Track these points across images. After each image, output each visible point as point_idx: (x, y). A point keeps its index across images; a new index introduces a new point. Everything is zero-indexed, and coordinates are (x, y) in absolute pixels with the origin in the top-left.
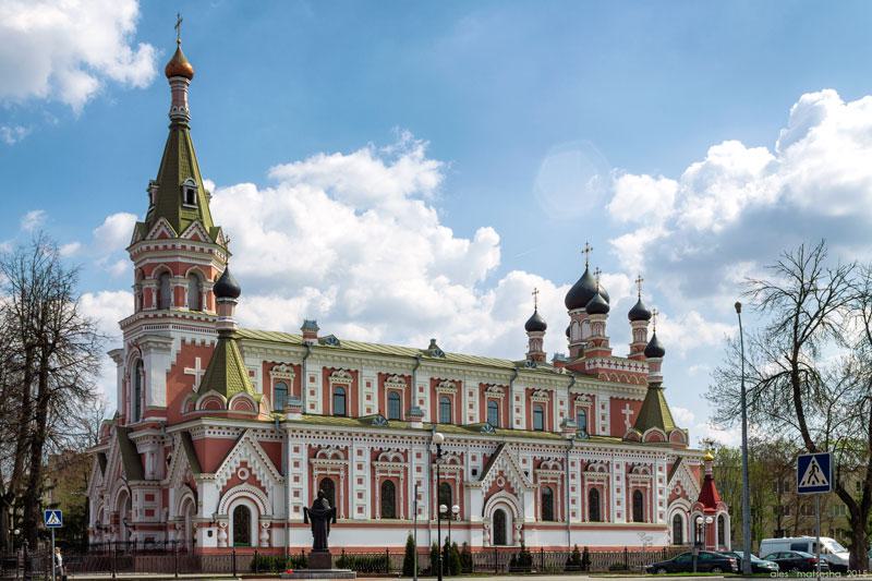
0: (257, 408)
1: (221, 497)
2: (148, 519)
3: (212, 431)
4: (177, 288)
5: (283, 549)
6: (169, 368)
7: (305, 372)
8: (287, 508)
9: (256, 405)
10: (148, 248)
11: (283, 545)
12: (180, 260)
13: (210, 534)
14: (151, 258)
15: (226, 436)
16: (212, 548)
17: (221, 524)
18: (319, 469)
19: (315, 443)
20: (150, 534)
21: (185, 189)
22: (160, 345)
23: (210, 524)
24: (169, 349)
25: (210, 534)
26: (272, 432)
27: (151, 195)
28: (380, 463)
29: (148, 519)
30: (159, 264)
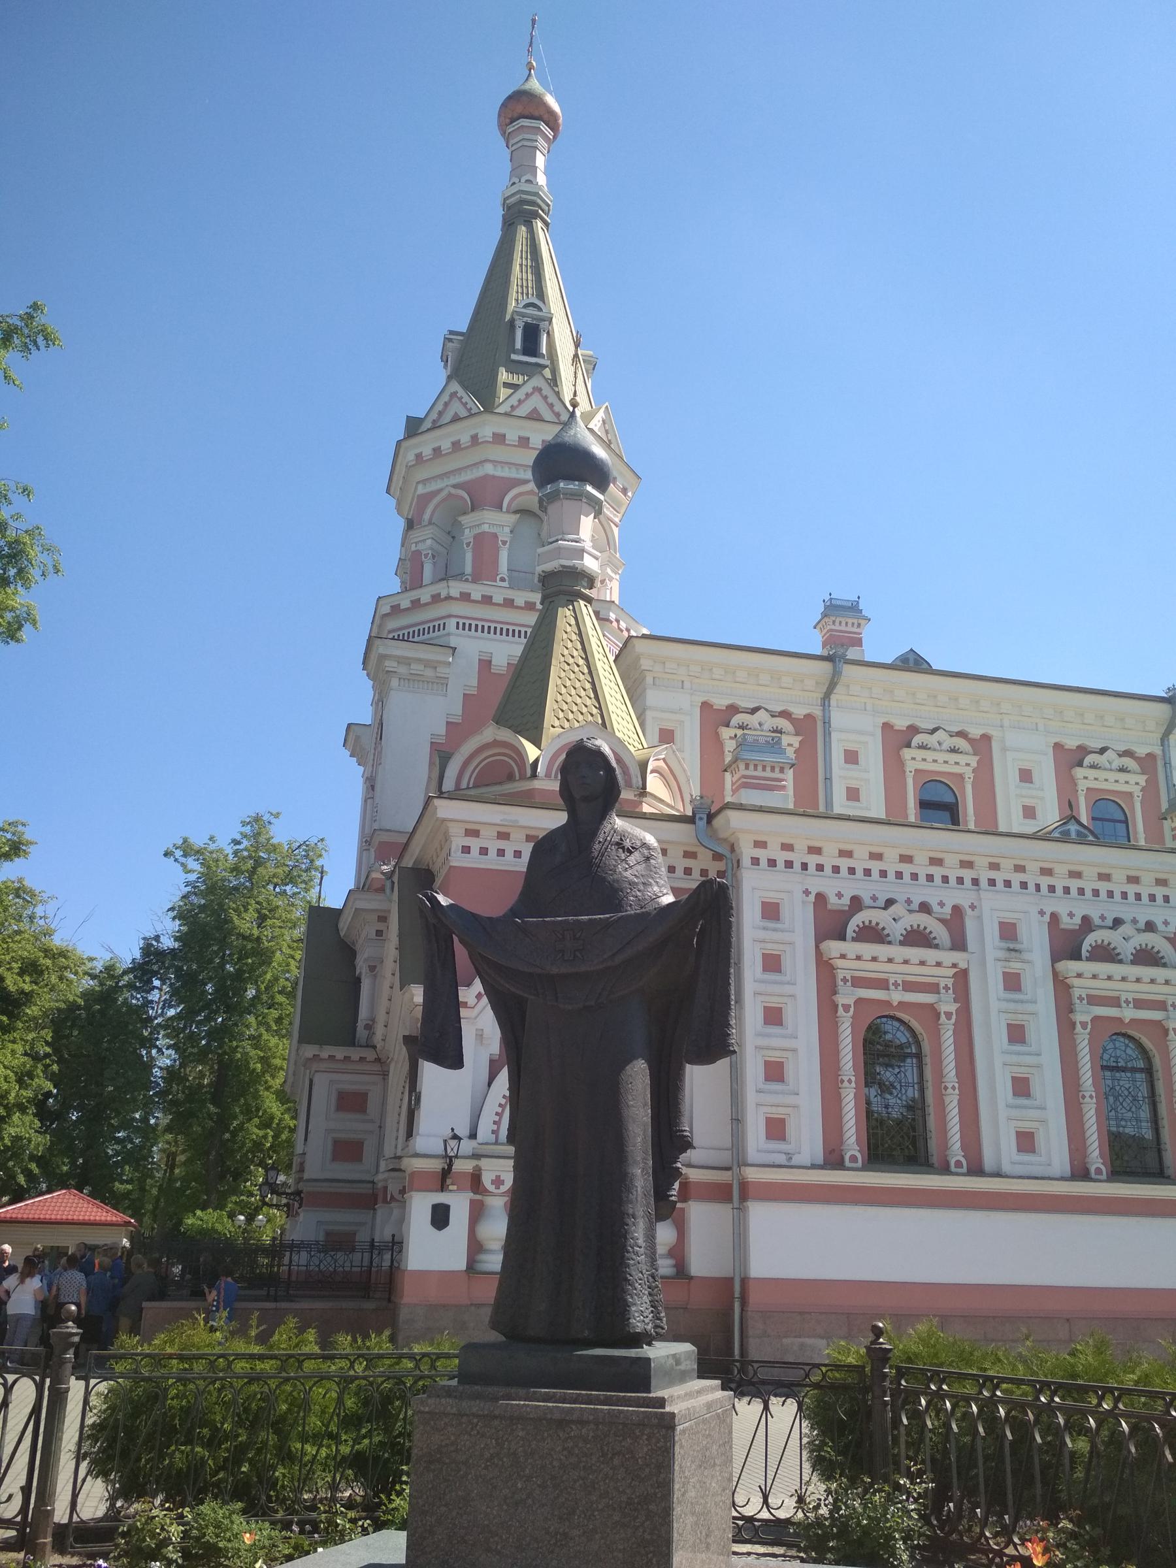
0: (636, 780)
1: (489, 1085)
2: (345, 1170)
3: (475, 844)
4: (480, 538)
5: (729, 1281)
6: (442, 730)
7: (827, 734)
8: (737, 1120)
9: (634, 771)
10: (419, 456)
11: (729, 1274)
12: (489, 469)
13: (440, 1216)
14: (424, 482)
15: (491, 862)
16: (446, 1276)
17: (487, 1179)
18: (858, 982)
19: (839, 890)
20: (341, 1219)
21: (520, 324)
22: (416, 668)
23: (443, 1179)
24: (443, 682)
25: (440, 1216)
26: (688, 855)
27: (445, 367)
28: (1087, 967)
29: (345, 1170)
30: (440, 491)
